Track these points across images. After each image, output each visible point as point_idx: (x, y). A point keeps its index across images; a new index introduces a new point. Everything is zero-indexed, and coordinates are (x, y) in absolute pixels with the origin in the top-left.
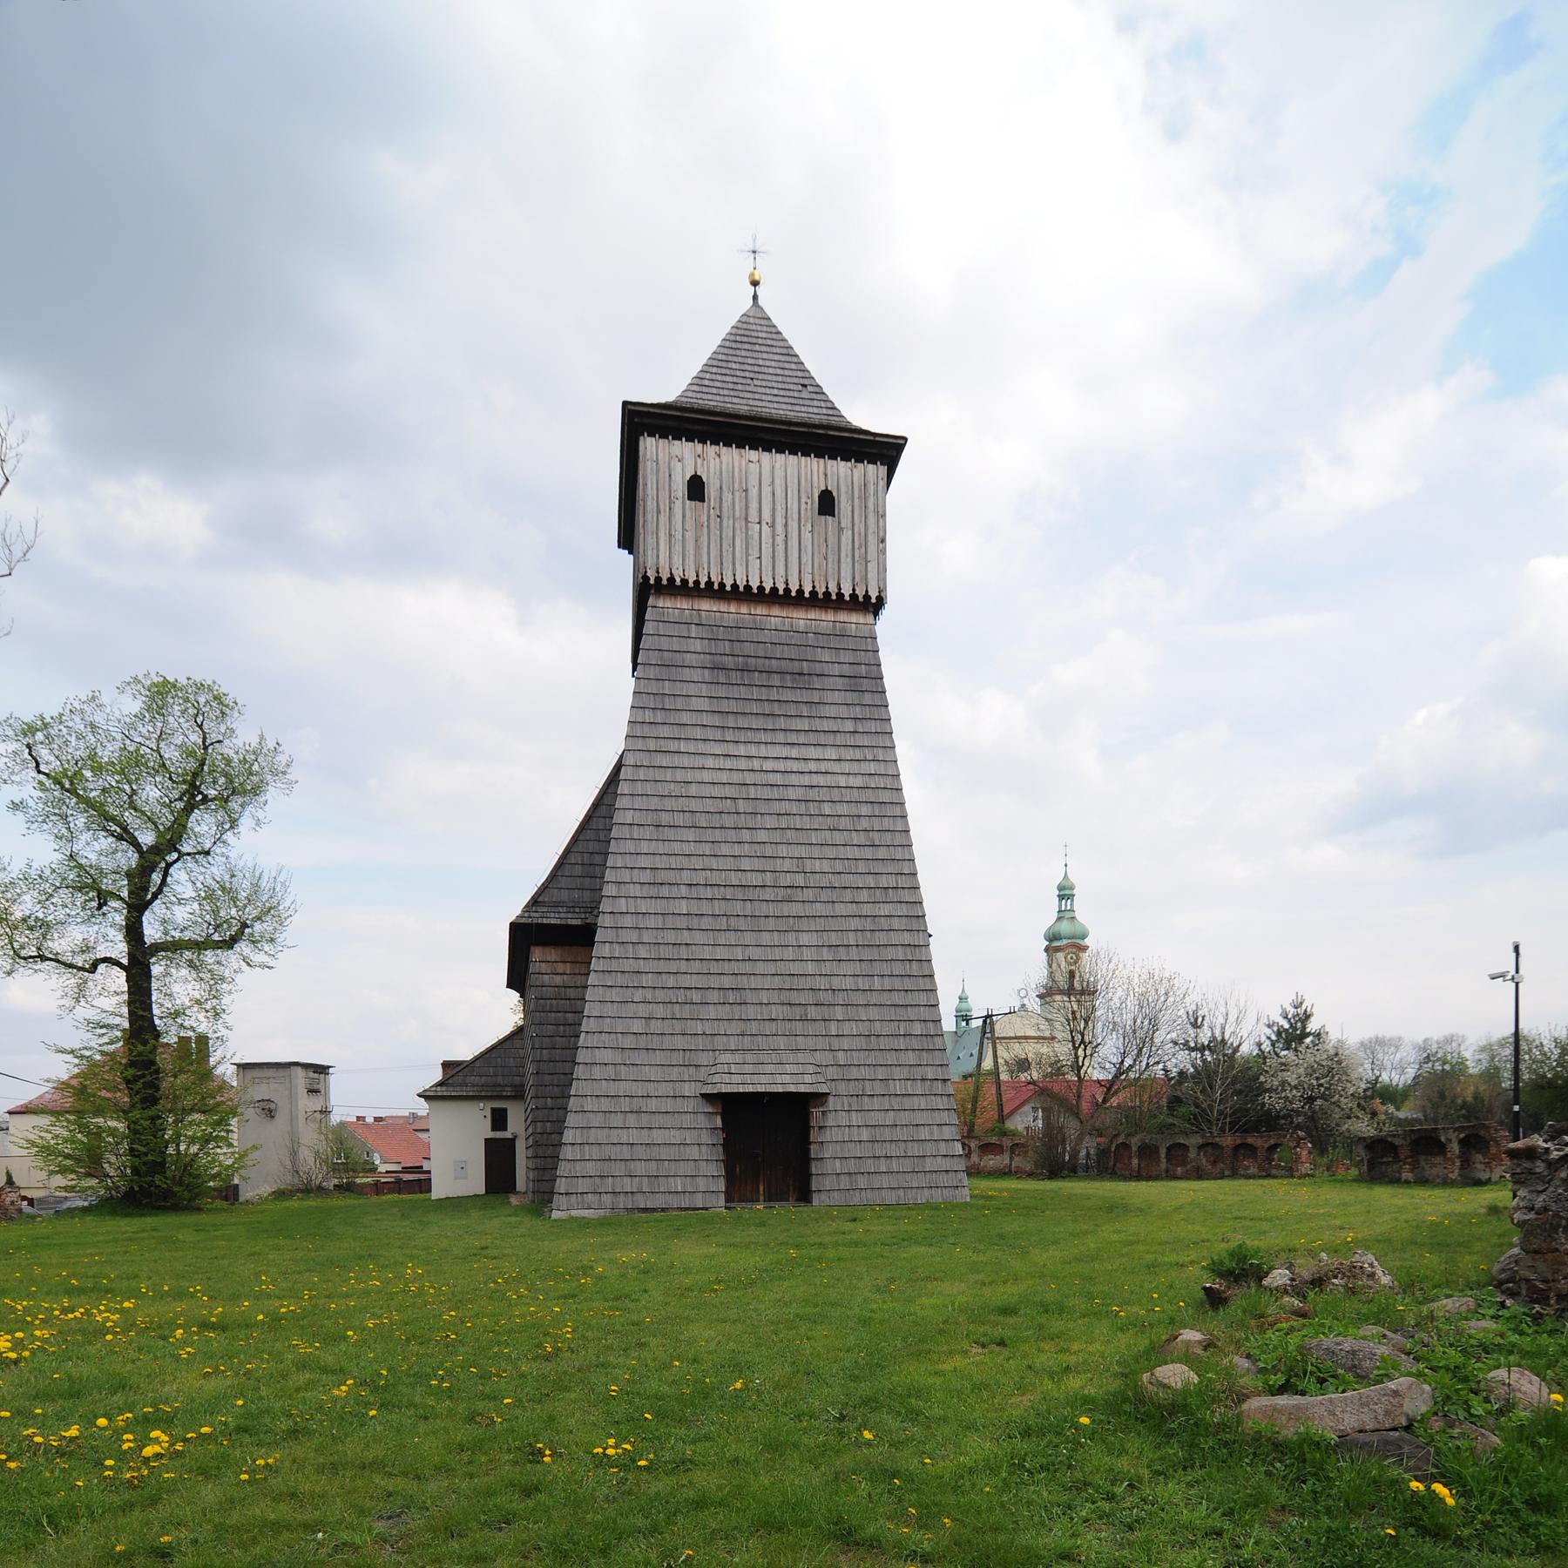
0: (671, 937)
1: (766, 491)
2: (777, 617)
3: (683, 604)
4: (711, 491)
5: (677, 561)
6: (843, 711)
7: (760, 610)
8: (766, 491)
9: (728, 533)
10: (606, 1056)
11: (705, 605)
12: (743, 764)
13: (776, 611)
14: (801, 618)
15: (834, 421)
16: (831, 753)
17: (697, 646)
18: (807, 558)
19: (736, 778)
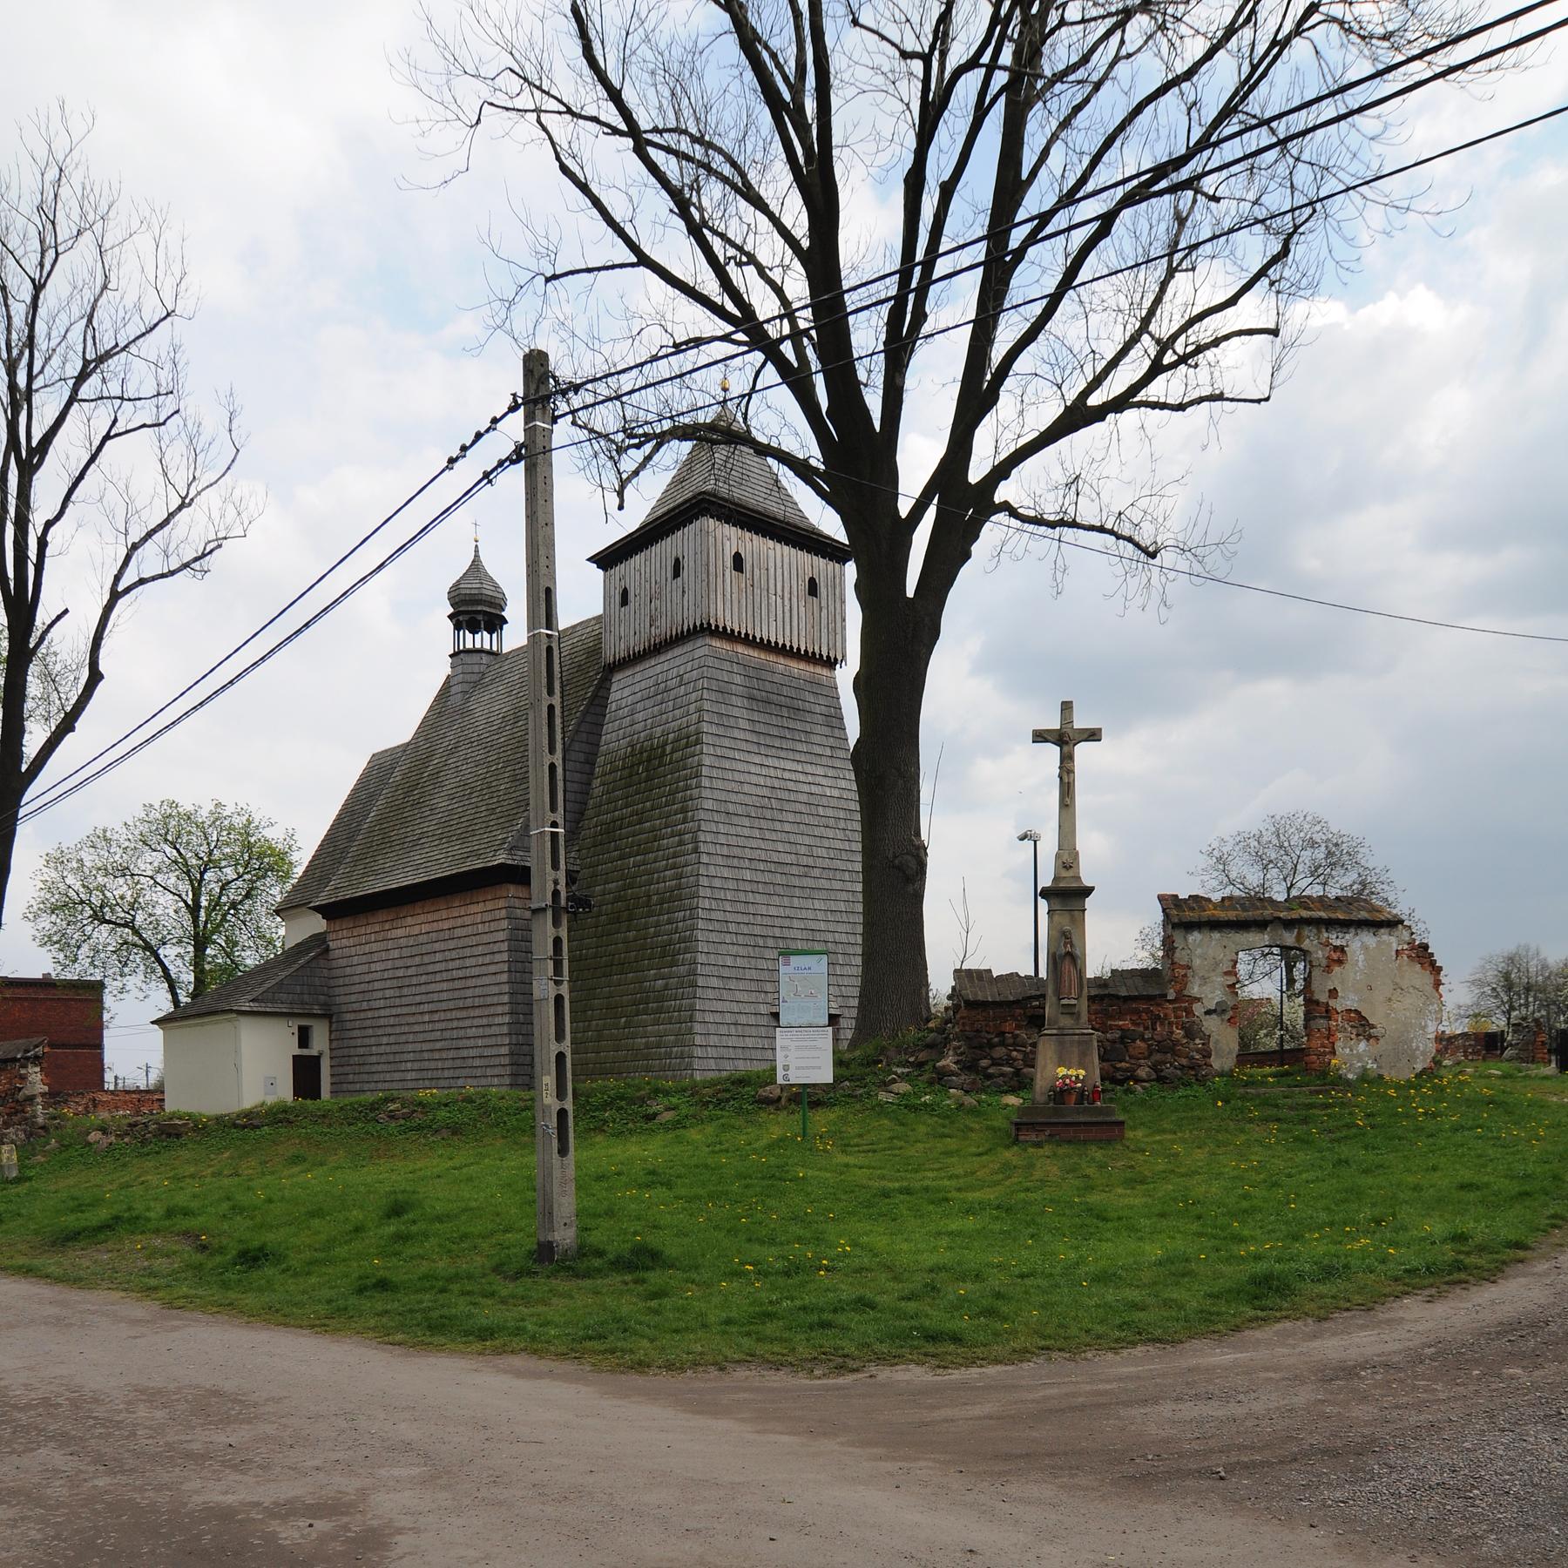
0: (742, 897)
1: (779, 571)
2: (781, 664)
3: (727, 646)
4: (747, 566)
5: (728, 617)
6: (824, 741)
7: (772, 658)
8: (779, 571)
9: (757, 599)
10: (715, 982)
11: (740, 649)
12: (772, 772)
13: (781, 660)
14: (797, 667)
15: (796, 520)
16: (820, 771)
17: (738, 679)
18: (802, 625)
19: (769, 782)
